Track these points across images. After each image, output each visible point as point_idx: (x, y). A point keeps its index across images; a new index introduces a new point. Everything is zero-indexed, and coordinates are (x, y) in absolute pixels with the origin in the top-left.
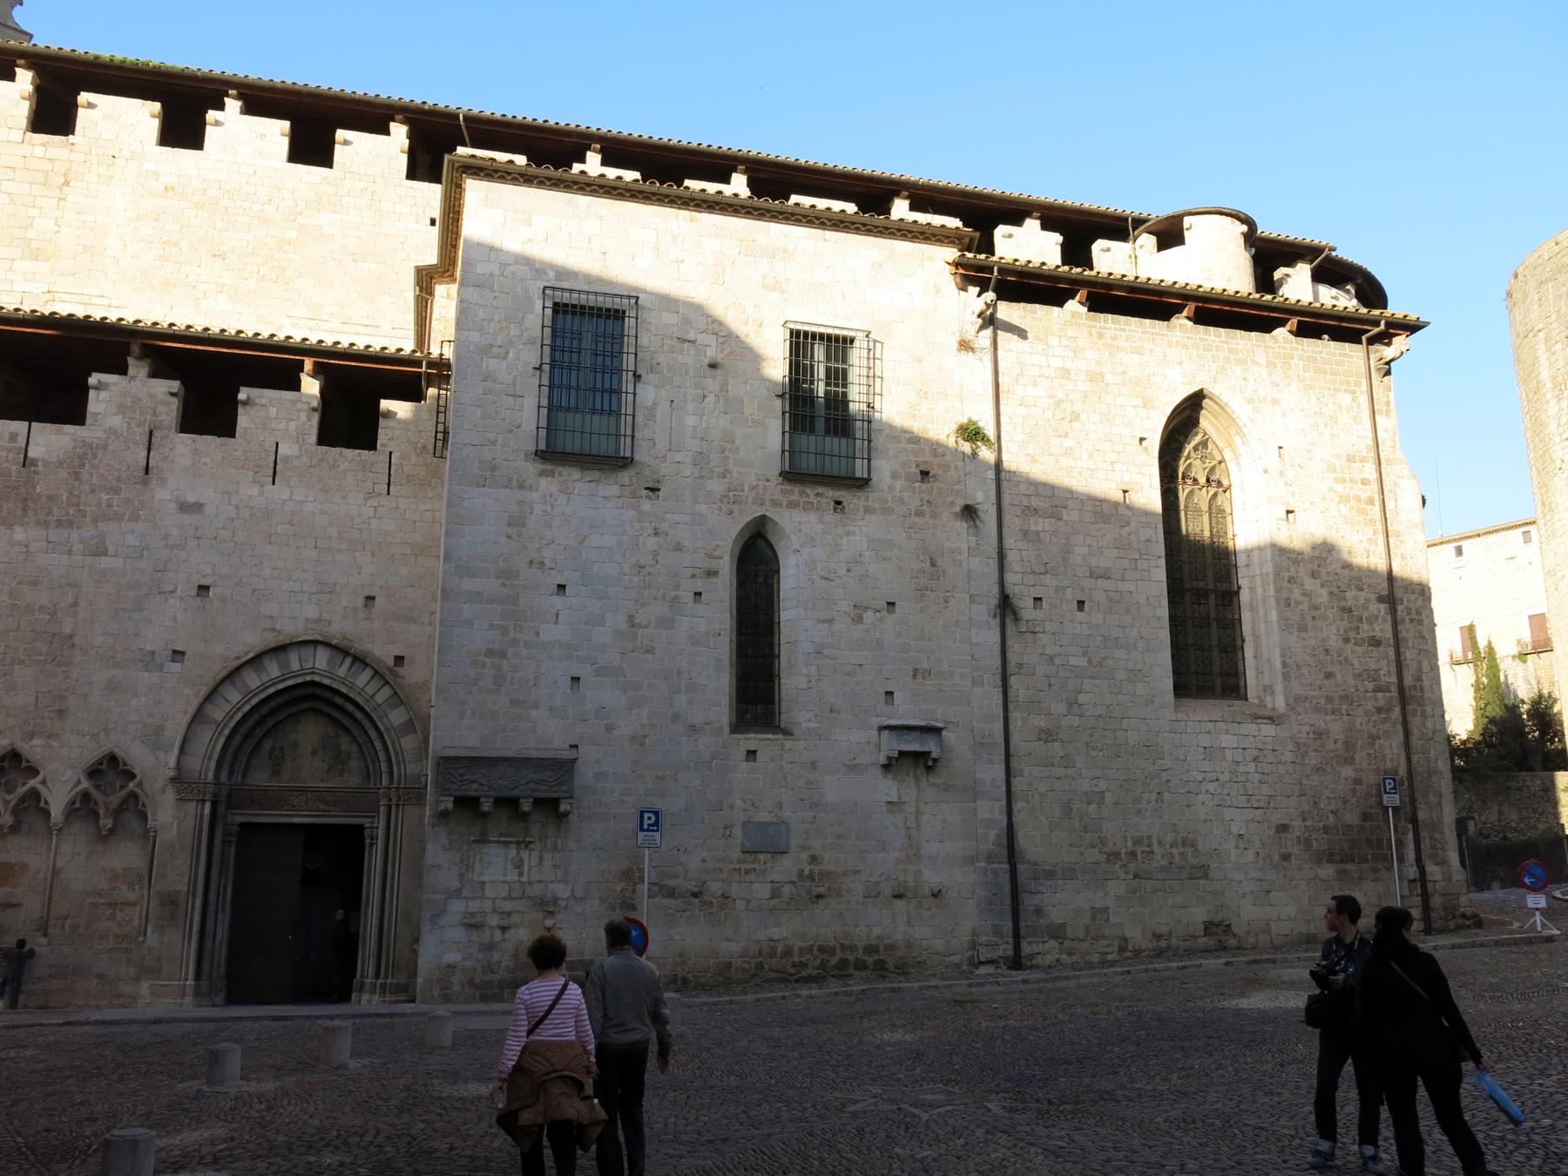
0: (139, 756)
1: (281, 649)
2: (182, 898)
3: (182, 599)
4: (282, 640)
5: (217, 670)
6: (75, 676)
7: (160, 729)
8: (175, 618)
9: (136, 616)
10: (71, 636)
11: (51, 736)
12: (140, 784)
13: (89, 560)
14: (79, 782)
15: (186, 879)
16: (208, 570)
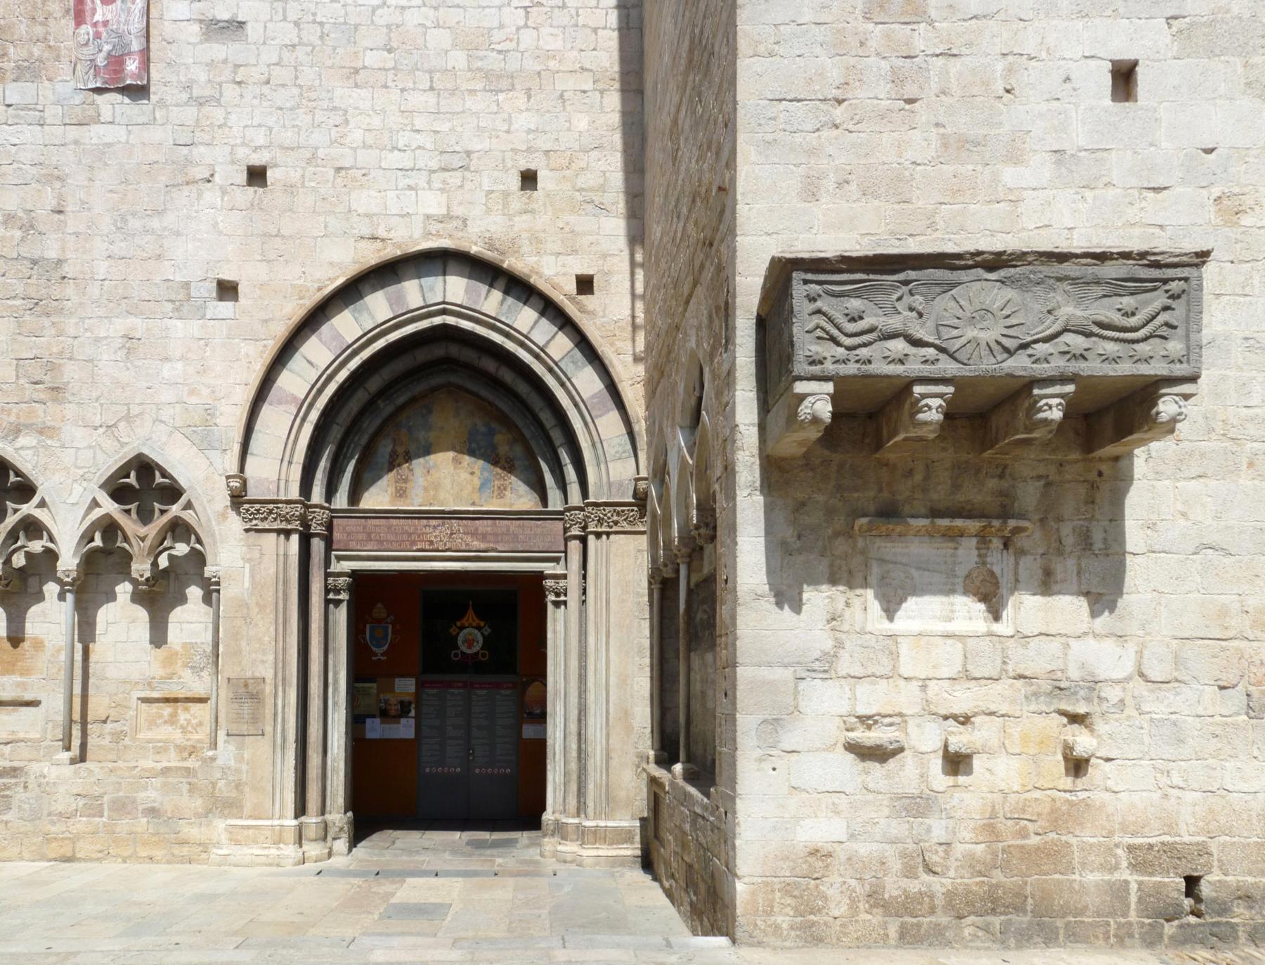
0: (180, 460)
1: (387, 272)
2: (268, 689)
3: (224, 192)
4: (390, 252)
5: (295, 310)
6: (71, 331)
7: (210, 412)
8: (215, 225)
9: (155, 223)
10: (59, 262)
11: (43, 431)
12: (189, 506)
13: (73, 132)
14: (95, 504)
15: (271, 657)
16: (261, 141)
